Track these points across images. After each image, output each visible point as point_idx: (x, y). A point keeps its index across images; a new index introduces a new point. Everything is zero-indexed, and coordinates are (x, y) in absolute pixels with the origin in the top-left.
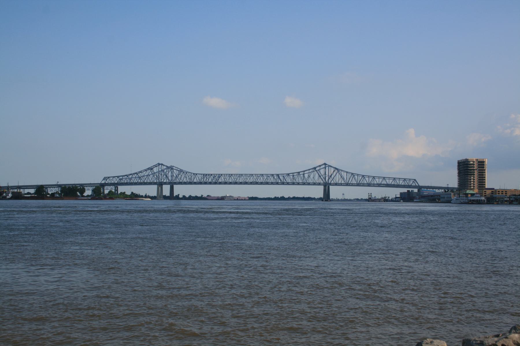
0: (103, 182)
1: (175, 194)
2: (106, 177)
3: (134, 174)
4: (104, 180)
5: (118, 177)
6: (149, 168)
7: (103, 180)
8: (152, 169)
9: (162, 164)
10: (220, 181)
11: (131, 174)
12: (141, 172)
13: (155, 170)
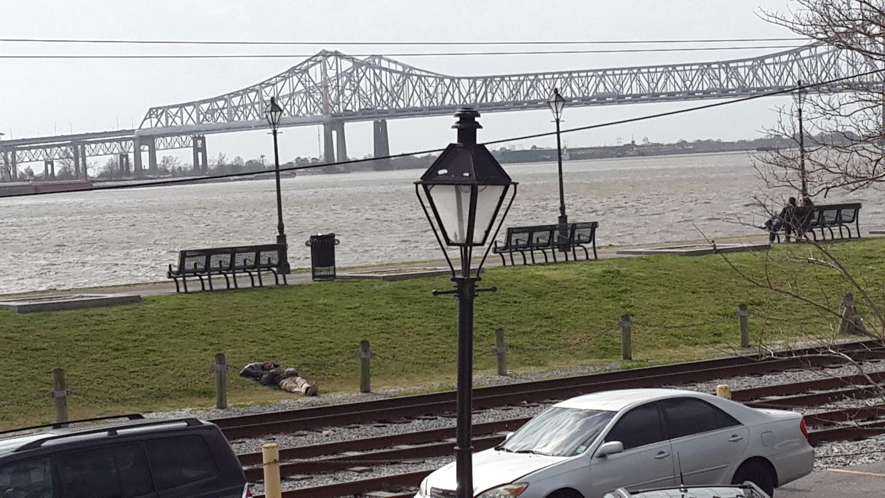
0: (147, 125)
1: (394, 150)
2: (157, 109)
3: (246, 91)
4: (150, 117)
5: (196, 104)
6: (294, 68)
7: (145, 119)
8: (306, 71)
9: (337, 54)
10: (534, 97)
11: (236, 94)
12: (268, 85)
13: (315, 73)
